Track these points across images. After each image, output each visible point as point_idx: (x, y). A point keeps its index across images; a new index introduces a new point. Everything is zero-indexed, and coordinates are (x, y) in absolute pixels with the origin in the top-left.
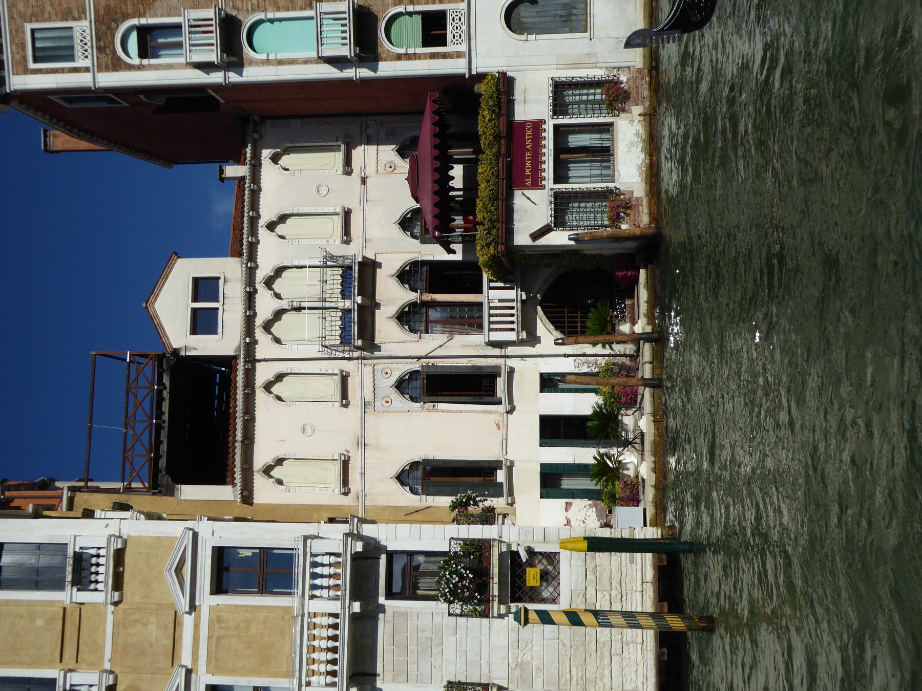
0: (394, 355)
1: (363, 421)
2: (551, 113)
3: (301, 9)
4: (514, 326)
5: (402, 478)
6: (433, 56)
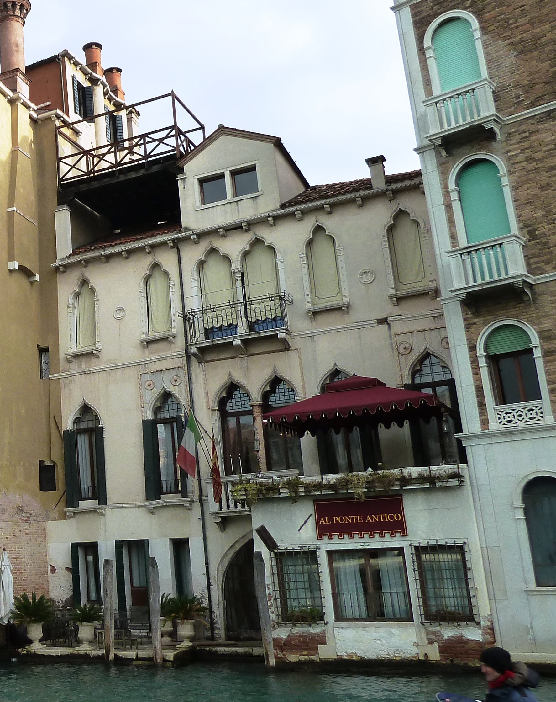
0: (194, 386)
1: (129, 366)
2: (416, 543)
3: (519, 216)
4: (225, 509)
5: (86, 409)
6: (479, 390)
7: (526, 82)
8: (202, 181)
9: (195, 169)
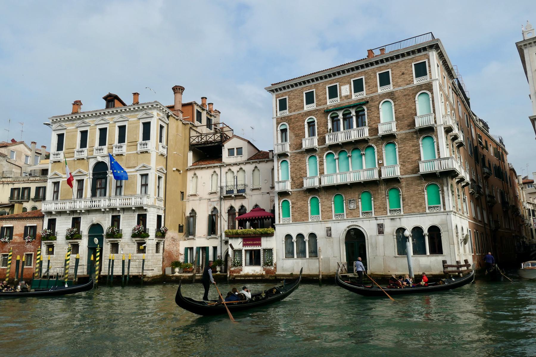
1: (205, 199)
6: (279, 214)
8: (229, 149)
9: (227, 146)
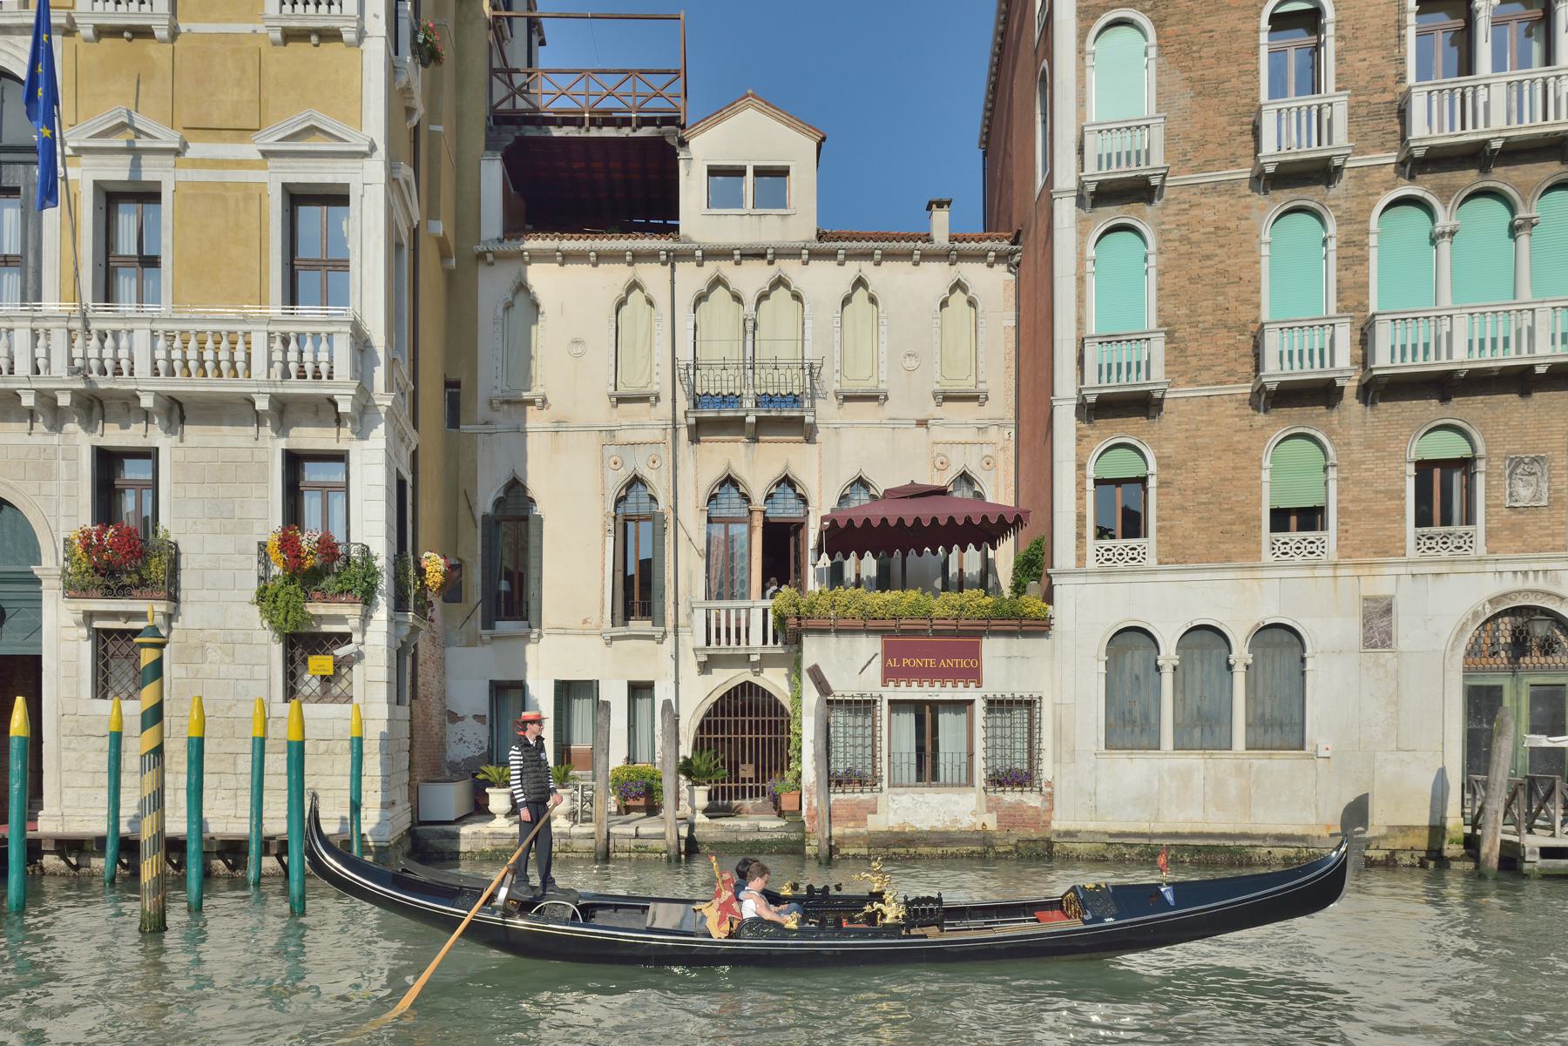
1: (588, 429)
3: (1159, 310)
7: (1197, 136)
